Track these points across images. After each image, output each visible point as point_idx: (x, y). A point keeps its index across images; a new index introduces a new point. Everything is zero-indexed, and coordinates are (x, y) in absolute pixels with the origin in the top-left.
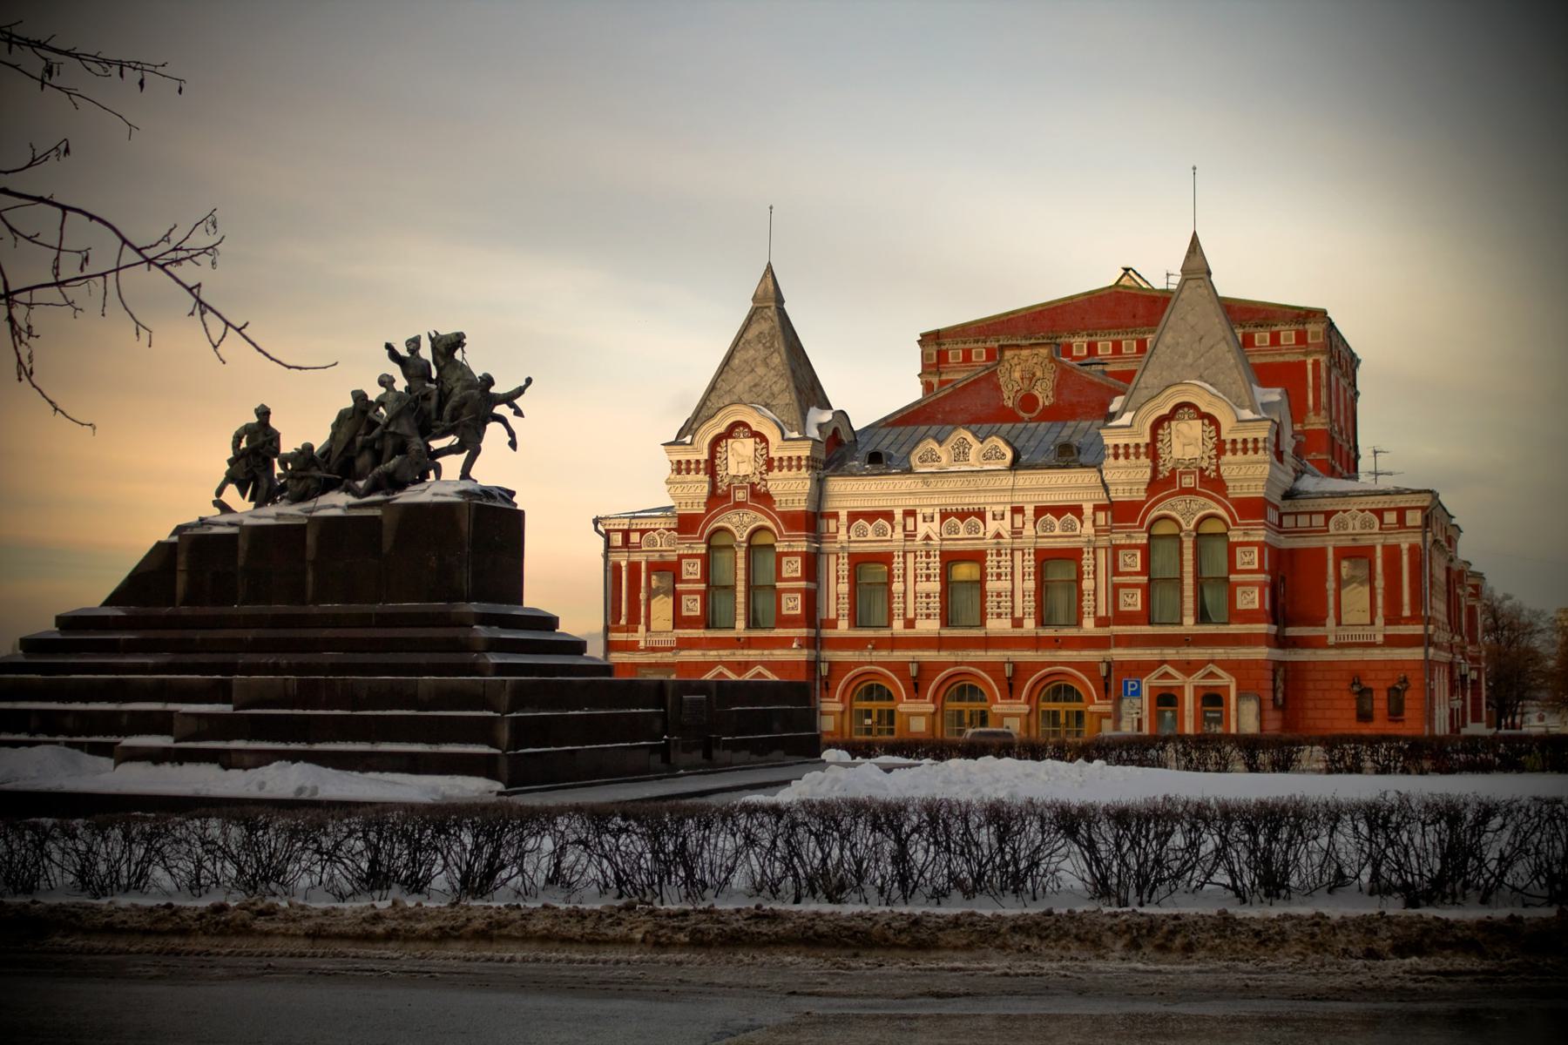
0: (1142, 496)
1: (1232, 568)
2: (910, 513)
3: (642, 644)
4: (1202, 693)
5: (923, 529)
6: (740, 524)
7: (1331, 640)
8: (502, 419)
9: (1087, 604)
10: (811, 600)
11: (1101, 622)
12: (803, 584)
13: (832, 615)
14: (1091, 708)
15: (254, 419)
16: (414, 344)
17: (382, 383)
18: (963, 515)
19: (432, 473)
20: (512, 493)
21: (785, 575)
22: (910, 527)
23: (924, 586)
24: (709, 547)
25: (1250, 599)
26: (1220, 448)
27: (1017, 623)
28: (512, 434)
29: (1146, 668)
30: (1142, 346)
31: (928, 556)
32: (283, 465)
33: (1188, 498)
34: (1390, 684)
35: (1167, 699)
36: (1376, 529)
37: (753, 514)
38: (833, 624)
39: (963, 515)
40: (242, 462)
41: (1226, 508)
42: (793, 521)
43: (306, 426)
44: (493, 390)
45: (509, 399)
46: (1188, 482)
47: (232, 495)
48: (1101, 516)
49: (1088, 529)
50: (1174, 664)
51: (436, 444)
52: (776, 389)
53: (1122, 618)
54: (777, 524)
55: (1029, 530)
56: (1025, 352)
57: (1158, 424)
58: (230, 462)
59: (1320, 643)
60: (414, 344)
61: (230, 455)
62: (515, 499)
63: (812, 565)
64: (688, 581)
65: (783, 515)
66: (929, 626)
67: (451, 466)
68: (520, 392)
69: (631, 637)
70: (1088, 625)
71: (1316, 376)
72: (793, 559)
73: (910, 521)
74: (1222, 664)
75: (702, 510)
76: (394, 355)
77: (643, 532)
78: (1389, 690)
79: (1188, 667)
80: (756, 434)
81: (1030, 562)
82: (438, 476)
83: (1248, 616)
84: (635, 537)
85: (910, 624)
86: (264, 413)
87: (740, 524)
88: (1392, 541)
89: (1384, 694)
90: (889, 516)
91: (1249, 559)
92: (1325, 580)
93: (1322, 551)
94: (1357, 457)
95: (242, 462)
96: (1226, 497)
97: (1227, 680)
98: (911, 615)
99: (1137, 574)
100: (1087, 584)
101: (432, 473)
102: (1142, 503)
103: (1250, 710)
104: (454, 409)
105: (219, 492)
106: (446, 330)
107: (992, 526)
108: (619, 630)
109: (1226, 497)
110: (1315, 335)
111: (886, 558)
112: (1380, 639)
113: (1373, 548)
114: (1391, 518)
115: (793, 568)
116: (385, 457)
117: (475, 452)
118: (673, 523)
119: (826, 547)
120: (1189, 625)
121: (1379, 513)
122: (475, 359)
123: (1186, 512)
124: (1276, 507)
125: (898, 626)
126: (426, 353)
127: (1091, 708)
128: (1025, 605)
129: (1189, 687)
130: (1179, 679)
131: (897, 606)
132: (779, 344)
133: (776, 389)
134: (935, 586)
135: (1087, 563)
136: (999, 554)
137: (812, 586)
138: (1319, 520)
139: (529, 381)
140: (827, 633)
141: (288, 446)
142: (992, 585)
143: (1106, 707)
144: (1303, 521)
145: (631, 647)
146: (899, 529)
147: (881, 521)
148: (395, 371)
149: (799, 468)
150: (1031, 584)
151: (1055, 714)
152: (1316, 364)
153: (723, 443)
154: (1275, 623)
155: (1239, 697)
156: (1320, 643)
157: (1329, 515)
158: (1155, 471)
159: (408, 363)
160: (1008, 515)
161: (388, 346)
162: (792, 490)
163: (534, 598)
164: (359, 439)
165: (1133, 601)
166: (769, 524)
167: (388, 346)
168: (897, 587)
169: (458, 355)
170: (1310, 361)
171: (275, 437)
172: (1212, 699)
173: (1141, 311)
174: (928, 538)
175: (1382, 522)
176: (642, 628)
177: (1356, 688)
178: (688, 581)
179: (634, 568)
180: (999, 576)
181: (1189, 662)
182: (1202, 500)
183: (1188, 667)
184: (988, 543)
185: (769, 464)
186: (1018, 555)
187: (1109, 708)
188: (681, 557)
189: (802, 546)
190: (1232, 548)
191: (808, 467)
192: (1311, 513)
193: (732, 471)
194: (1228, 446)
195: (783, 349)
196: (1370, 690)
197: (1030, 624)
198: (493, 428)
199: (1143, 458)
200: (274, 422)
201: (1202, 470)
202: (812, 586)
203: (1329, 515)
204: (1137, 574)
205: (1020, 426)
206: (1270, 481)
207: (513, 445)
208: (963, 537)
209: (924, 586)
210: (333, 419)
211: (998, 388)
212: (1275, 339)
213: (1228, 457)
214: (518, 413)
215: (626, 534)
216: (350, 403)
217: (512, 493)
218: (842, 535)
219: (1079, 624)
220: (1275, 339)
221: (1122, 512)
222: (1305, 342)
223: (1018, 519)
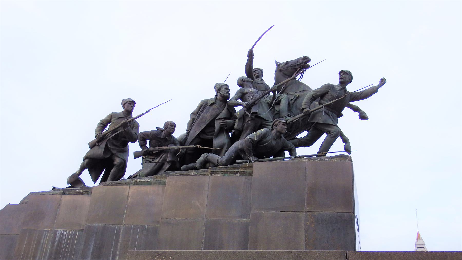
15: (120, 110)
44: (351, 88)
58: (92, 146)
61: (92, 138)
68: (372, 92)
86: (129, 105)
106: (291, 55)
139: (383, 82)
210: (194, 107)
214: (363, 117)
216: (211, 94)
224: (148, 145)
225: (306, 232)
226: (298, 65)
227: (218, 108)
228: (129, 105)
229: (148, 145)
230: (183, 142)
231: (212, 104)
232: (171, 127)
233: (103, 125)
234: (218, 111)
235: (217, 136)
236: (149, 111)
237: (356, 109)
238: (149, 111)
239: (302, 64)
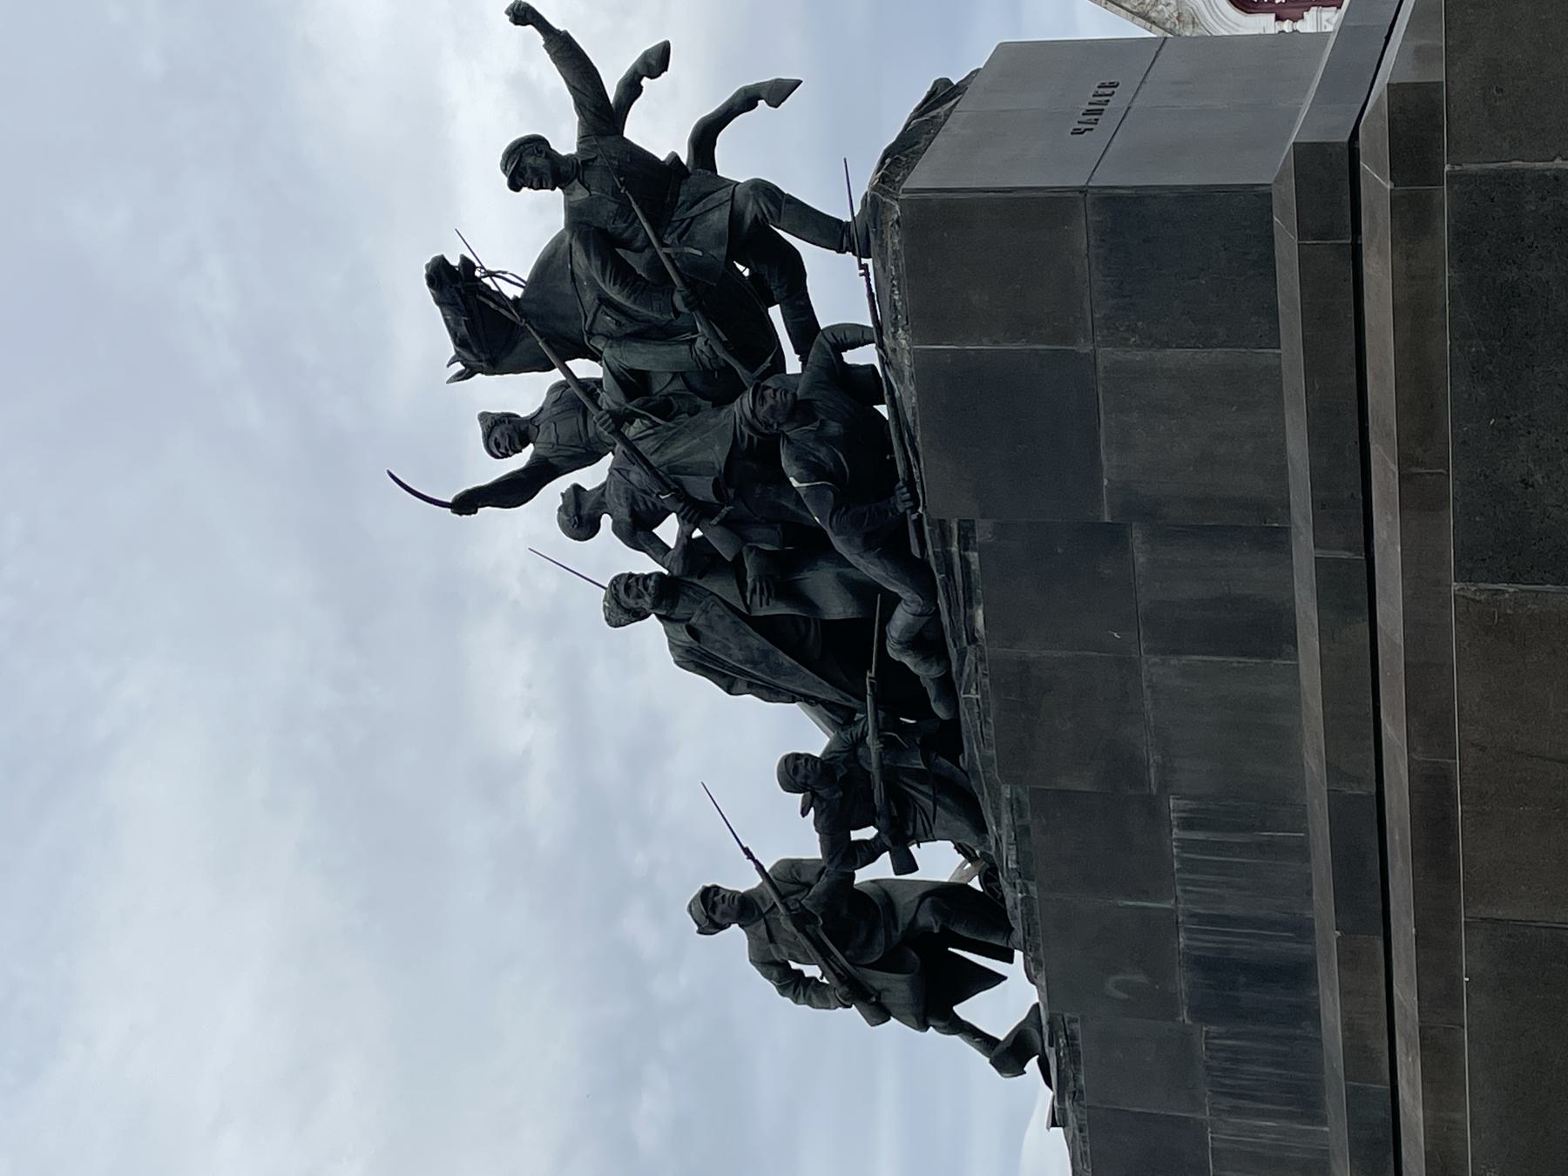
8: (705, 137)
19: (851, 357)
28: (746, 101)
43: (733, 768)
44: (565, 139)
58: (879, 1012)
68: (565, 50)
76: (511, 492)
86: (714, 910)
101: (851, 357)
106: (427, 332)
126: (524, 393)
148: (553, 493)
171: (788, 879)
207: (778, 92)
214: (657, 62)
224: (869, 833)
225: (1167, 345)
226: (465, 303)
227: (705, 611)
228: (714, 910)
229: (869, 833)
230: (838, 716)
231: (692, 631)
232: (797, 773)
234: (717, 611)
235: (810, 605)
236: (747, 851)
237: (632, 89)
238: (747, 851)
239: (456, 285)
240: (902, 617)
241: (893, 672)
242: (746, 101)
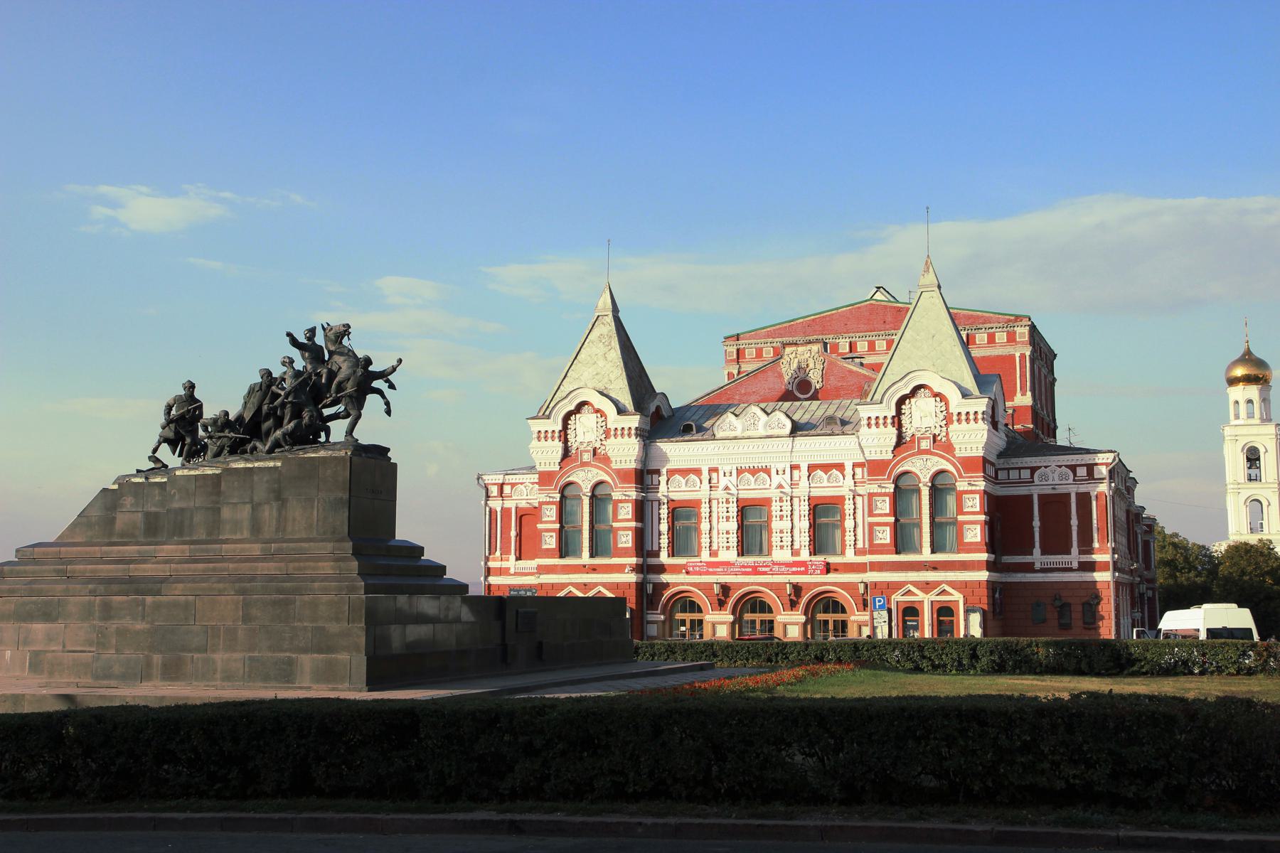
0: (890, 456)
1: (960, 511)
2: (713, 470)
3: (512, 571)
4: (936, 607)
5: (724, 481)
6: (585, 479)
7: (1038, 566)
9: (849, 538)
10: (640, 535)
11: (858, 552)
12: (633, 524)
13: (656, 548)
14: (853, 618)
16: (312, 331)
17: (284, 364)
18: (754, 471)
19: (323, 434)
20: (388, 450)
21: (620, 517)
22: (714, 481)
23: (724, 526)
24: (563, 497)
25: (975, 534)
26: (948, 420)
27: (795, 553)
28: (387, 404)
29: (893, 587)
30: (890, 343)
31: (727, 502)
32: (206, 430)
33: (925, 457)
34: (1084, 600)
35: (911, 611)
36: (1071, 481)
37: (595, 471)
38: (657, 554)
39: (754, 471)
40: (172, 426)
41: (954, 465)
42: (623, 475)
43: (224, 398)
44: (371, 368)
45: (382, 375)
46: (925, 445)
47: (165, 453)
48: (858, 471)
49: (849, 482)
50: (915, 584)
51: (327, 412)
52: (612, 377)
53: (874, 549)
54: (613, 479)
55: (804, 483)
56: (800, 349)
57: (901, 402)
59: (1029, 568)
60: (312, 331)
62: (389, 455)
63: (641, 510)
64: (546, 522)
65: (618, 472)
66: (731, 555)
67: (338, 430)
69: (505, 564)
70: (850, 552)
71: (1023, 367)
72: (625, 505)
73: (714, 475)
74: (952, 584)
75: (557, 468)
76: (294, 342)
77: (513, 485)
78: (1083, 604)
79: (927, 587)
80: (597, 411)
81: (805, 508)
82: (328, 435)
83: (971, 548)
84: (507, 489)
85: (713, 553)
86: (191, 387)
87: (585, 479)
88: (1083, 489)
89: (1080, 608)
90: (697, 472)
91: (974, 503)
92: (1032, 520)
93: (1030, 497)
94: (1055, 427)
95: (172, 426)
96: (954, 456)
97: (957, 596)
98: (715, 547)
99: (886, 515)
100: (849, 524)
101: (323, 434)
102: (889, 462)
103: (976, 619)
104: (340, 384)
105: (155, 451)
106: (336, 321)
107: (776, 479)
108: (494, 560)
109: (954, 456)
110: (1022, 335)
111: (696, 504)
112: (1075, 565)
113: (1069, 495)
114: (1082, 472)
115: (626, 511)
116: (286, 421)
117: (359, 417)
118: (535, 478)
119: (651, 496)
120: (926, 555)
121: (1073, 468)
122: (359, 345)
123: (923, 468)
124: (993, 464)
125: (705, 556)
127: (853, 618)
128: (803, 539)
129: (926, 601)
130: (920, 595)
131: (705, 540)
132: (615, 343)
133: (612, 377)
134: (733, 525)
135: (848, 506)
136: (781, 500)
137: (640, 525)
138: (1026, 474)
139: (400, 361)
140: (652, 561)
141: (209, 412)
142: (776, 525)
143: (864, 617)
144: (1014, 475)
145: (502, 572)
146: (705, 482)
147: (692, 477)
148: (295, 354)
149: (629, 435)
150: (805, 524)
151: (826, 622)
152: (1023, 356)
153: (573, 418)
154: (993, 552)
155: (967, 612)
156: (1029, 568)
157: (1033, 470)
158: (900, 437)
159: (308, 348)
160: (788, 471)
161: (289, 335)
162: (626, 452)
163: (405, 531)
164: (265, 408)
165: (884, 536)
166: (609, 480)
167: (289, 335)
168: (705, 526)
169: (345, 341)
170: (1018, 355)
172: (944, 612)
173: (889, 319)
174: (727, 488)
175: (1075, 475)
176: (512, 557)
177: (1058, 603)
178: (546, 522)
179: (506, 512)
180: (781, 517)
181: (927, 583)
182: (936, 458)
183: (927, 587)
184: (774, 494)
185: (607, 433)
186: (796, 501)
187: (867, 618)
188: (541, 504)
189: (633, 494)
190: (960, 495)
191: (637, 435)
192: (1020, 469)
193: (579, 439)
194: (955, 418)
195: (618, 347)
196: (1070, 605)
197: (805, 555)
198: (372, 399)
199: (890, 426)
200: (197, 394)
201: (935, 436)
202: (640, 525)
203: (1033, 470)
204: (886, 515)
205: (798, 403)
206: (987, 446)
207: (388, 412)
208: (752, 489)
209: (724, 526)
210: (246, 391)
211: (781, 376)
212: (991, 339)
213: (954, 426)
215: (501, 486)
217: (388, 450)
218: (663, 488)
219: (843, 553)
220: (991, 339)
221: (875, 468)
222: (1014, 340)
223: (796, 473)
233: (169, 408)
240: (258, 445)
241: (249, 441)
242: (387, 404)
